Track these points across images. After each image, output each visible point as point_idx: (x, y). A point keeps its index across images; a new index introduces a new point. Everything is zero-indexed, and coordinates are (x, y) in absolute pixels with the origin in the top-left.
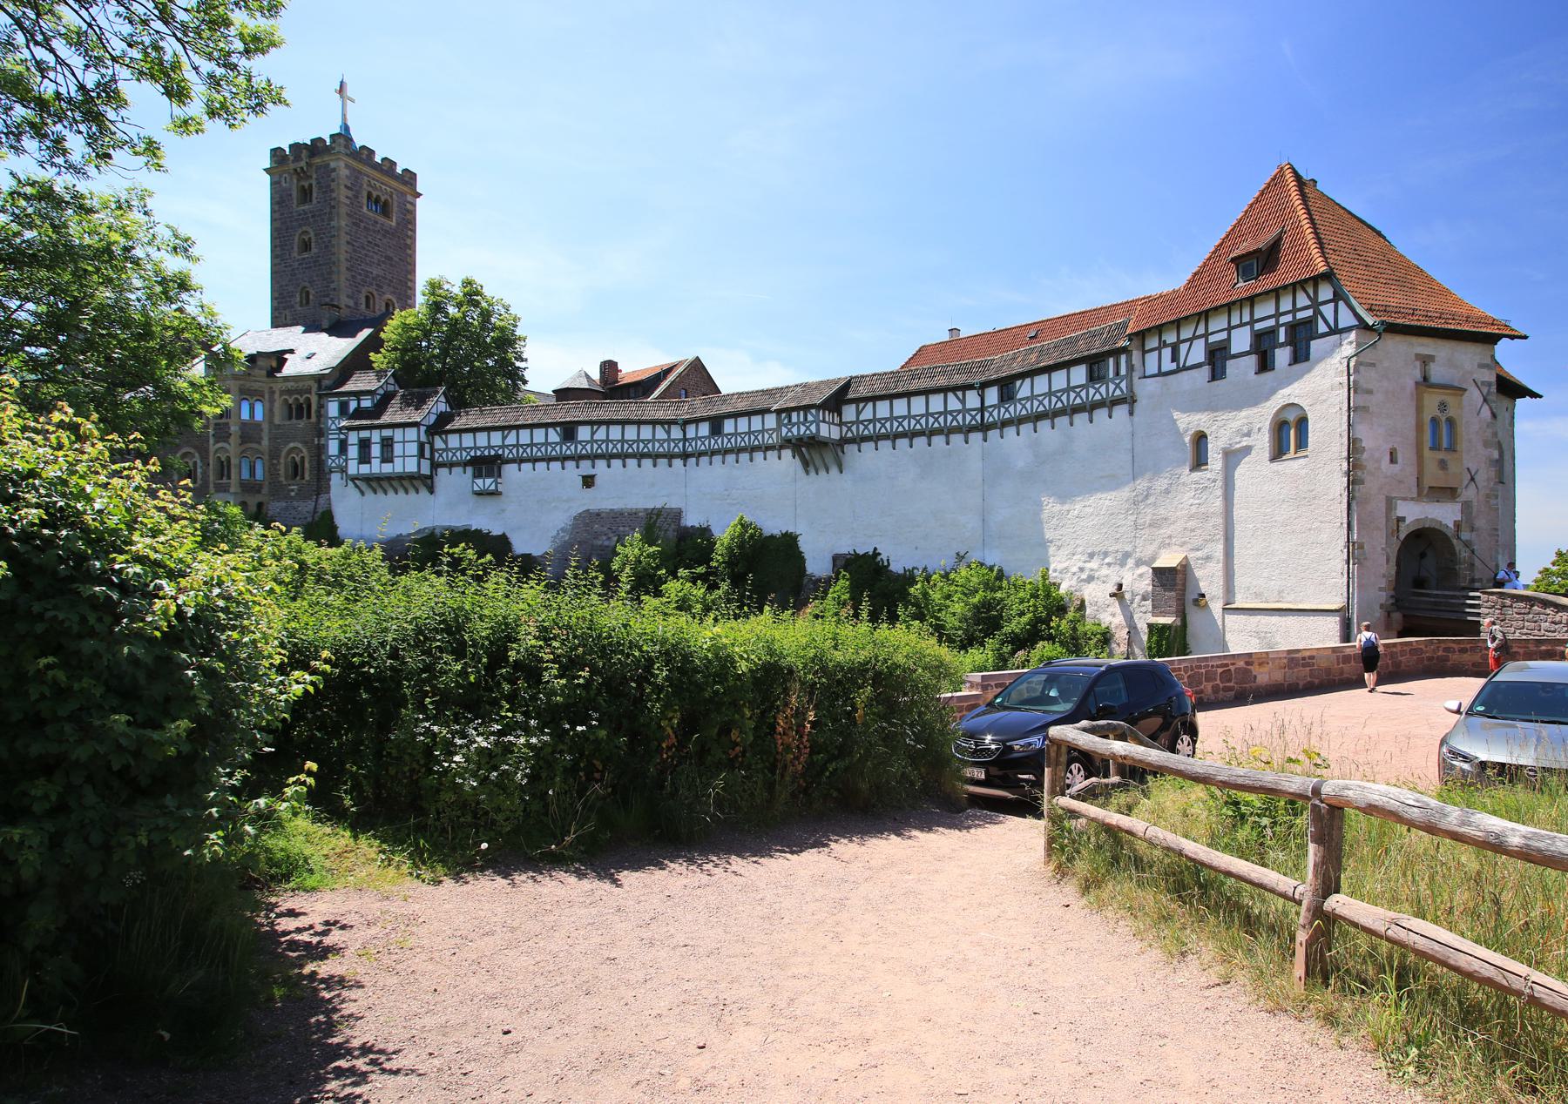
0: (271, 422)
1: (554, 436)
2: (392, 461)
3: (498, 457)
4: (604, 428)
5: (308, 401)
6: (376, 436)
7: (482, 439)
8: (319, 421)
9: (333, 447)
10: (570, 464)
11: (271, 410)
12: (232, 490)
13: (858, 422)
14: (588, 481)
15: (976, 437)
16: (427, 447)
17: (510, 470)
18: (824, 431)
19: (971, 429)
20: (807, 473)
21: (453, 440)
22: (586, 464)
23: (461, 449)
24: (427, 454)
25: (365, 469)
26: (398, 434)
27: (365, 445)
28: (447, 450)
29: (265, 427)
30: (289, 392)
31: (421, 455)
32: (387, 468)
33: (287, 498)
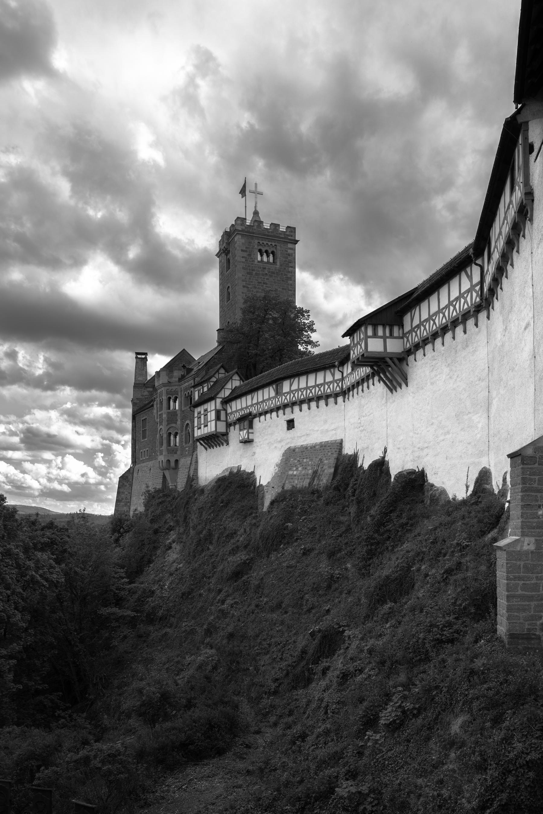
0: (181, 410)
1: (273, 394)
3: (250, 414)
4: (297, 379)
6: (201, 409)
10: (281, 412)
11: (181, 402)
13: (412, 330)
14: (291, 424)
15: (482, 316)
16: (223, 414)
17: (256, 420)
18: (375, 346)
19: (478, 309)
20: (391, 391)
22: (288, 410)
24: (223, 417)
29: (179, 413)
31: (218, 418)
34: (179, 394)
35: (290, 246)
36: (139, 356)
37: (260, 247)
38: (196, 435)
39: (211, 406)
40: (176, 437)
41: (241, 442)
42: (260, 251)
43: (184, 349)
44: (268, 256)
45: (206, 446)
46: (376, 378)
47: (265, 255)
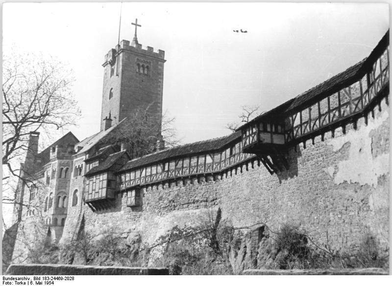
1: (160, 169)
3: (139, 185)
34: (71, 166)
35: (160, 63)
36: (33, 135)
37: (138, 63)
38: (86, 199)
39: (104, 177)
40: (64, 200)
41: (128, 206)
42: (138, 65)
43: (70, 134)
44: (144, 70)
45: (94, 208)
46: (256, 162)
47: (141, 68)
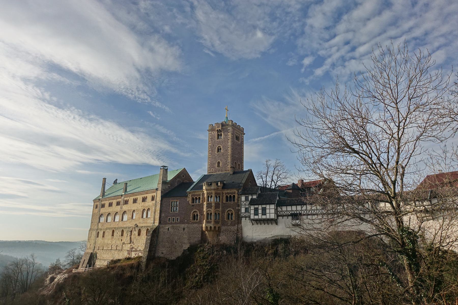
0: (222, 202)
2: (258, 215)
5: (234, 196)
6: (260, 207)
7: (294, 208)
8: (238, 202)
9: (243, 210)
12: (212, 223)
21: (284, 208)
23: (287, 211)
25: (256, 217)
26: (268, 207)
27: (256, 210)
28: (282, 211)
29: (221, 203)
30: (228, 193)
32: (264, 217)
33: (227, 225)
